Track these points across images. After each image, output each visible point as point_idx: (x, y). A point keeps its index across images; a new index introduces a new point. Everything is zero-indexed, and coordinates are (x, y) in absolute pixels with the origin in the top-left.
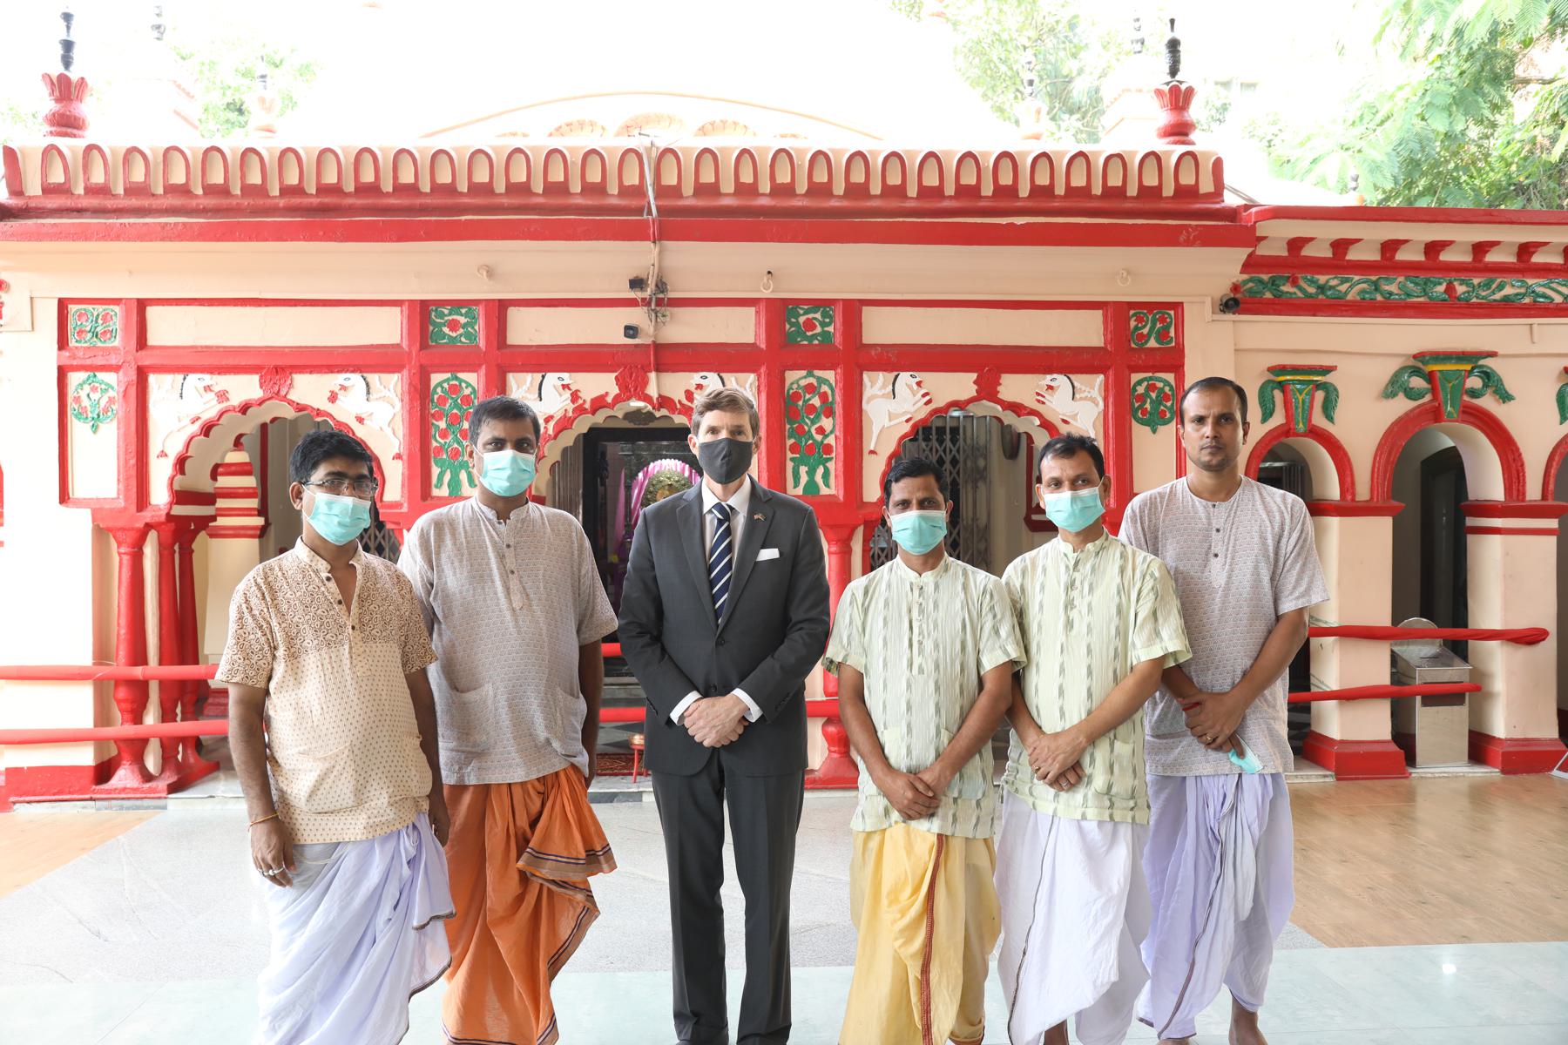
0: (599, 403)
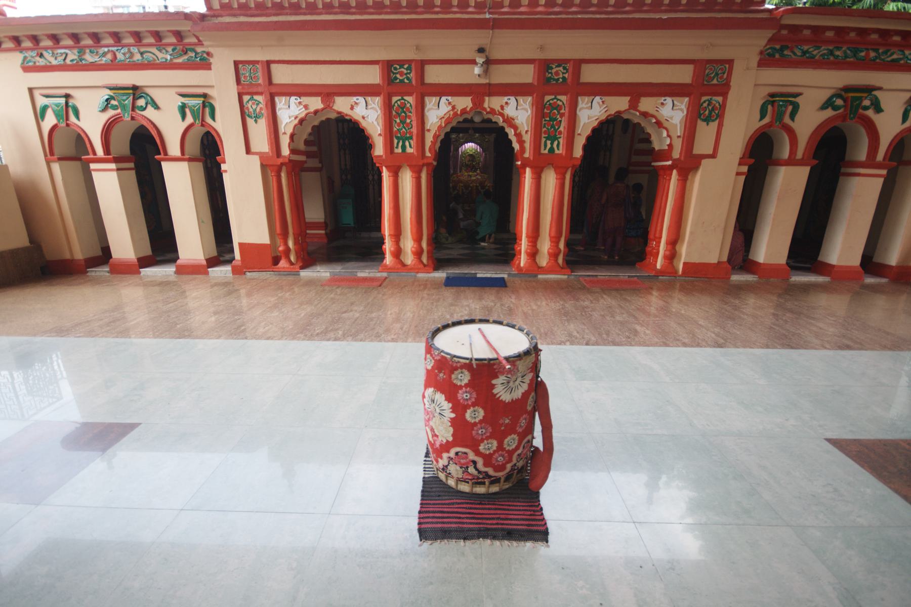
0: (464, 111)
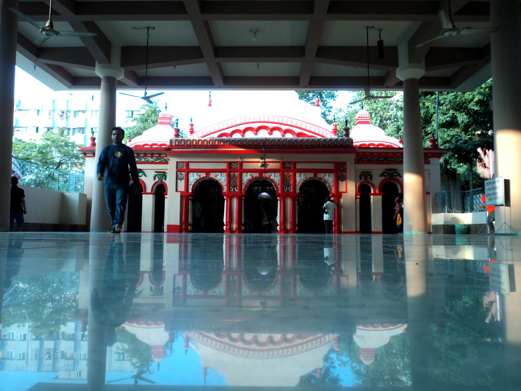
0: (256, 177)
